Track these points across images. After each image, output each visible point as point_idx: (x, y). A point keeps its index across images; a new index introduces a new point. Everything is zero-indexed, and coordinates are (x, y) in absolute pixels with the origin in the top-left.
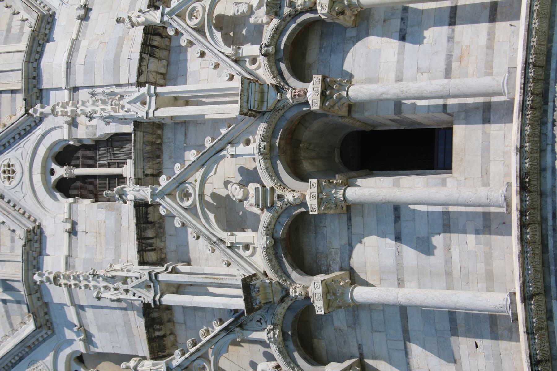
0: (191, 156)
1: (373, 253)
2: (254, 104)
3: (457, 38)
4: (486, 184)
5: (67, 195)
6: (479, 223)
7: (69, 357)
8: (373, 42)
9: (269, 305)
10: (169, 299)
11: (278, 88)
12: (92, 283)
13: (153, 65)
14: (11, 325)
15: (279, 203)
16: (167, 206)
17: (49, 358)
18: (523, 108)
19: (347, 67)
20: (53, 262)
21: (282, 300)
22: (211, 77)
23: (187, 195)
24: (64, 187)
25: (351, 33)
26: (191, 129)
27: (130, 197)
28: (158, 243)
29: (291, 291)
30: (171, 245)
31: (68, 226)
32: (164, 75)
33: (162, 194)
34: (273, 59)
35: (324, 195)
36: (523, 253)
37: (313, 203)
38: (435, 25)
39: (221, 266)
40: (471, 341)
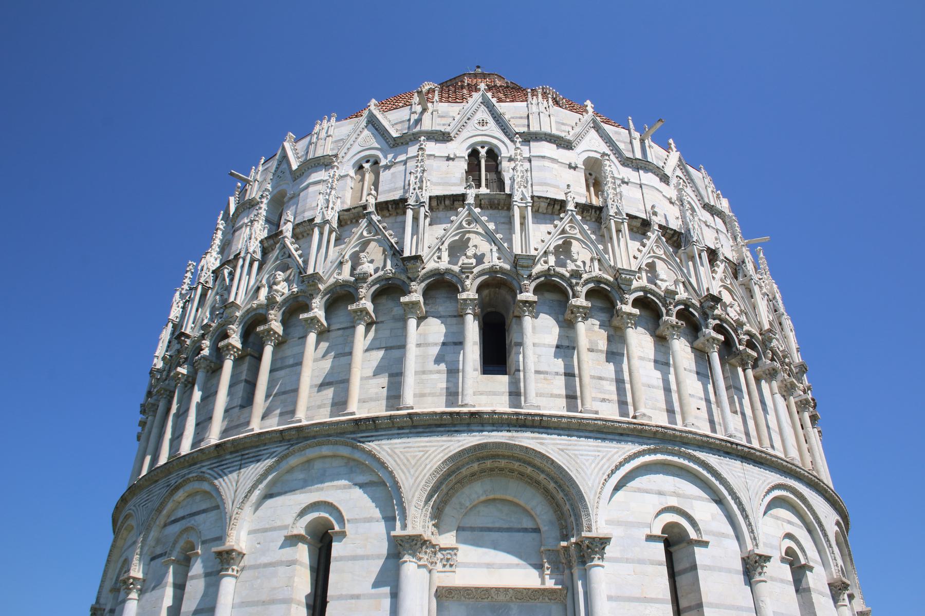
0: (491, 226)
1: (436, 330)
2: (521, 262)
4: (474, 394)
6: (453, 390)
7: (377, 156)
8: (556, 330)
9: (406, 270)
10: (410, 213)
11: (530, 276)
12: (419, 170)
13: (543, 205)
14: (396, 124)
15: (464, 276)
16: (463, 212)
17: (377, 146)
19: (542, 315)
20: (432, 147)
21: (409, 278)
22: (536, 238)
23: (469, 224)
24: (474, 154)
25: (561, 318)
26: (507, 226)
27: (468, 191)
28: (442, 207)
29: (413, 283)
30: (441, 214)
31: (452, 156)
32: (538, 211)
33: (470, 210)
34: (547, 274)
35: (469, 302)
36: (435, 414)
37: (464, 296)
38: (565, 365)
39: (428, 243)
40: (386, 385)
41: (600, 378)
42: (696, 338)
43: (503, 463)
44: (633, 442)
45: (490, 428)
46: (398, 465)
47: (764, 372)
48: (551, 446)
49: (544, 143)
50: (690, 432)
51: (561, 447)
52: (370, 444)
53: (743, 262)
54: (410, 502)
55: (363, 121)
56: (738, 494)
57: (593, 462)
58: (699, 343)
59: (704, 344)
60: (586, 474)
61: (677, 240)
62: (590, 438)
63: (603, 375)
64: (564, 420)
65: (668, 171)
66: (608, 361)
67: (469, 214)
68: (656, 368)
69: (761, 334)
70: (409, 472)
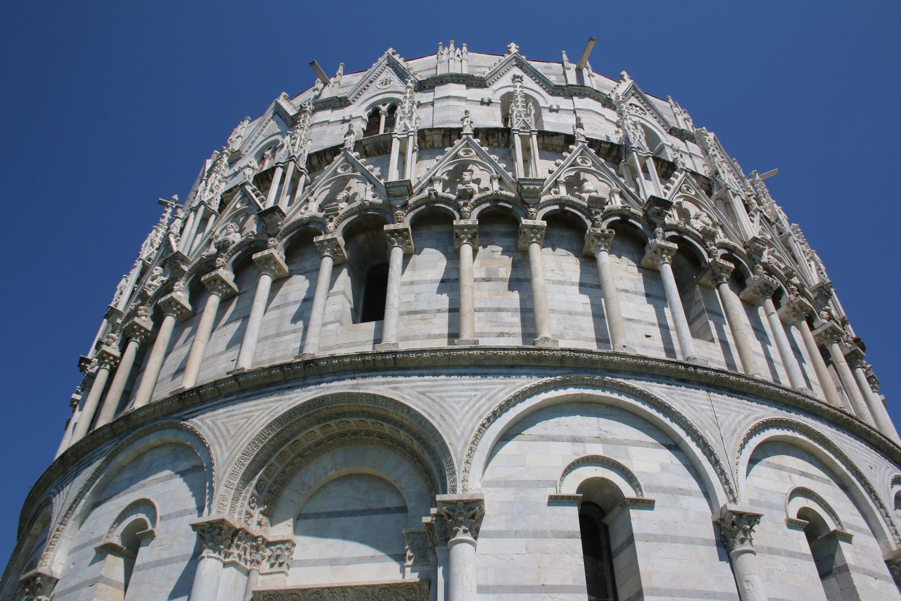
3: (438, 315)
5: (370, 116)
11: (405, 206)
38: (450, 300)
41: (499, 310)
42: (643, 253)
43: (353, 423)
44: (529, 375)
45: (331, 378)
46: (216, 438)
47: (754, 291)
48: (408, 391)
49: (451, 84)
51: (421, 390)
52: (193, 420)
53: (717, 173)
54: (220, 480)
55: (269, 113)
56: (701, 432)
57: (467, 403)
58: (646, 261)
59: (652, 259)
60: (454, 420)
61: (612, 153)
62: (465, 374)
63: (503, 306)
66: (511, 288)
67: (346, 160)
68: (581, 292)
69: (745, 247)
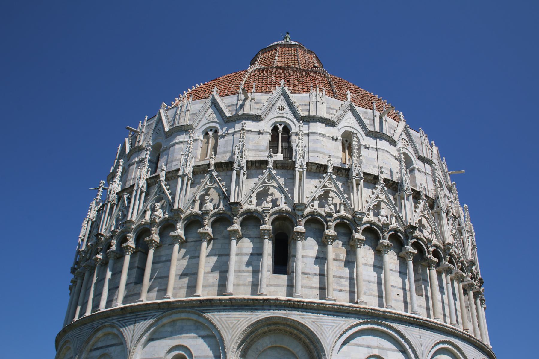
0: (282, 183)
1: (247, 245)
2: (297, 207)
3: (315, 276)
4: (267, 285)
5: (272, 130)
6: (255, 283)
7: (217, 128)
8: (316, 247)
9: (231, 210)
10: (234, 173)
11: (302, 216)
12: (241, 143)
13: (314, 168)
14: (229, 106)
15: (264, 215)
16: (266, 172)
17: (217, 120)
18: (290, 301)
19: (309, 238)
20: (250, 125)
21: (233, 214)
22: (309, 189)
23: (269, 181)
24: (275, 129)
25: (320, 240)
26: (292, 181)
27: (270, 159)
28: (254, 167)
29: (235, 218)
30: (253, 171)
31: (261, 131)
32: (311, 171)
33: (270, 172)
34: (312, 214)
35: (266, 232)
36: (244, 299)
37: (263, 227)
39: (245, 192)
40: (218, 278)
41: (340, 277)
42: (401, 251)
43: (281, 327)
44: (355, 318)
45: (275, 308)
46: (223, 327)
47: (443, 269)
48: (308, 320)
49: (318, 124)
50: (389, 312)
51: (313, 320)
52: (208, 314)
54: (229, 349)
55: (209, 101)
56: (415, 348)
57: (331, 329)
58: (402, 254)
59: (404, 255)
61: (394, 187)
62: (330, 315)
63: (342, 275)
64: (316, 305)
65: (396, 138)
66: (345, 266)
67: (269, 175)
68: (374, 270)
69: (443, 246)
70: (229, 332)
